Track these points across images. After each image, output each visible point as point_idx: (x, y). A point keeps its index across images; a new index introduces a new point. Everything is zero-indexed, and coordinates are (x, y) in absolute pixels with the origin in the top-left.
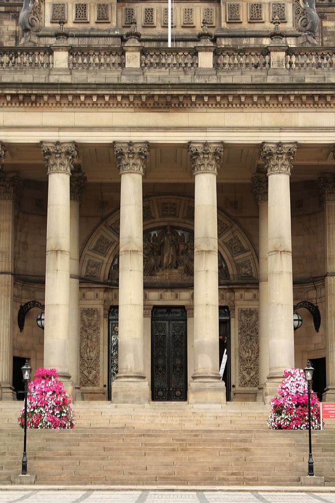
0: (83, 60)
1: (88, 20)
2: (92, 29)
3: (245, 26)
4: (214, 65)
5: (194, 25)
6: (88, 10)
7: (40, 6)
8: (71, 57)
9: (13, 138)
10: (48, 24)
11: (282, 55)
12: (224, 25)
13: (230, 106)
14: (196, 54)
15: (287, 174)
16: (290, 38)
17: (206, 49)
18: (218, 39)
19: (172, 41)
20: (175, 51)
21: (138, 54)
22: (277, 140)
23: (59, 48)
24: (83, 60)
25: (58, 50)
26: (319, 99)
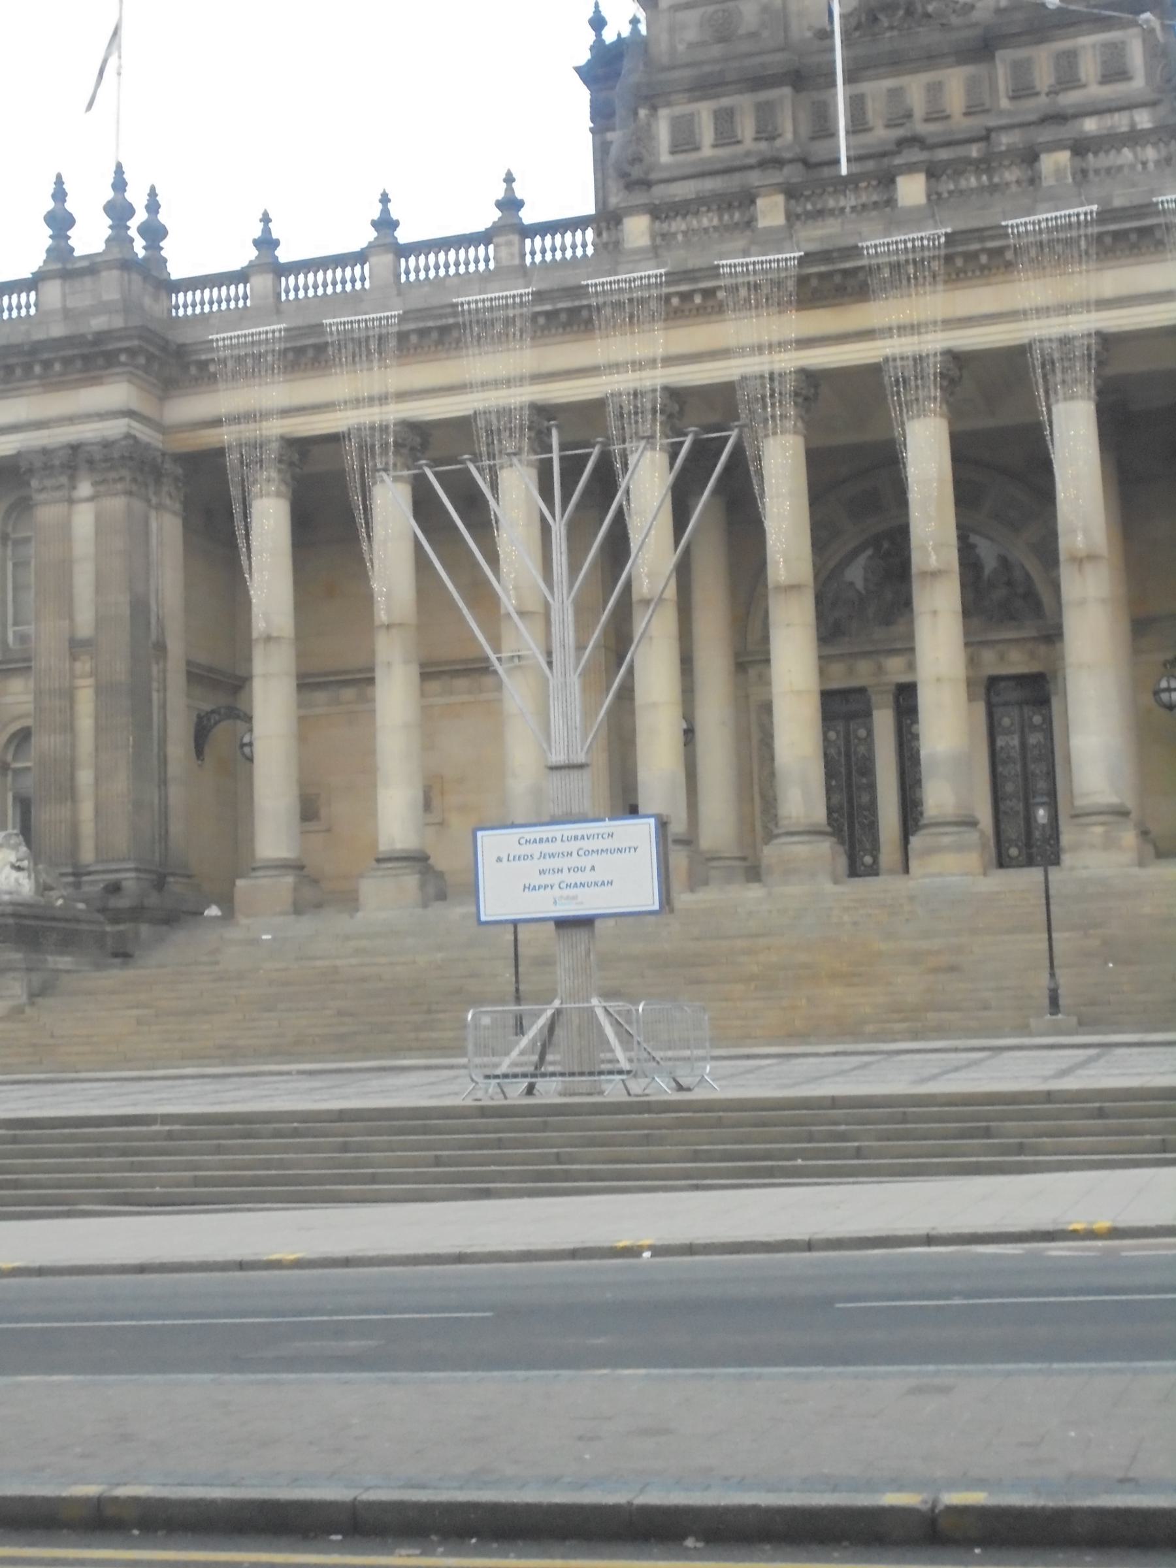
0: (732, 217)
1: (740, 138)
2: (748, 154)
3: (1096, 91)
4: (929, 196)
5: (948, 112)
6: (738, 118)
7: (649, 125)
8: (657, 223)
9: (556, 394)
10: (665, 158)
11: (1063, 157)
12: (1004, 103)
13: (962, 275)
14: (892, 181)
15: (1089, 398)
16: (1140, 110)
17: (910, 168)
18: (993, 135)
19: (849, 160)
20: (852, 181)
21: (780, 199)
22: (631, 386)
23: (633, 210)
24: (732, 217)
25: (631, 215)
26: (965, 261)
